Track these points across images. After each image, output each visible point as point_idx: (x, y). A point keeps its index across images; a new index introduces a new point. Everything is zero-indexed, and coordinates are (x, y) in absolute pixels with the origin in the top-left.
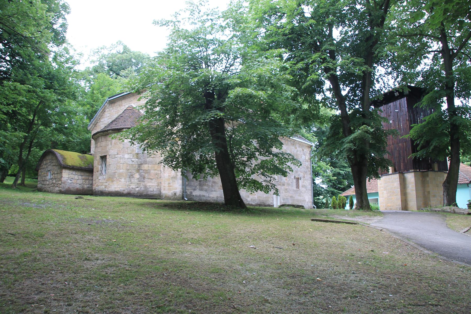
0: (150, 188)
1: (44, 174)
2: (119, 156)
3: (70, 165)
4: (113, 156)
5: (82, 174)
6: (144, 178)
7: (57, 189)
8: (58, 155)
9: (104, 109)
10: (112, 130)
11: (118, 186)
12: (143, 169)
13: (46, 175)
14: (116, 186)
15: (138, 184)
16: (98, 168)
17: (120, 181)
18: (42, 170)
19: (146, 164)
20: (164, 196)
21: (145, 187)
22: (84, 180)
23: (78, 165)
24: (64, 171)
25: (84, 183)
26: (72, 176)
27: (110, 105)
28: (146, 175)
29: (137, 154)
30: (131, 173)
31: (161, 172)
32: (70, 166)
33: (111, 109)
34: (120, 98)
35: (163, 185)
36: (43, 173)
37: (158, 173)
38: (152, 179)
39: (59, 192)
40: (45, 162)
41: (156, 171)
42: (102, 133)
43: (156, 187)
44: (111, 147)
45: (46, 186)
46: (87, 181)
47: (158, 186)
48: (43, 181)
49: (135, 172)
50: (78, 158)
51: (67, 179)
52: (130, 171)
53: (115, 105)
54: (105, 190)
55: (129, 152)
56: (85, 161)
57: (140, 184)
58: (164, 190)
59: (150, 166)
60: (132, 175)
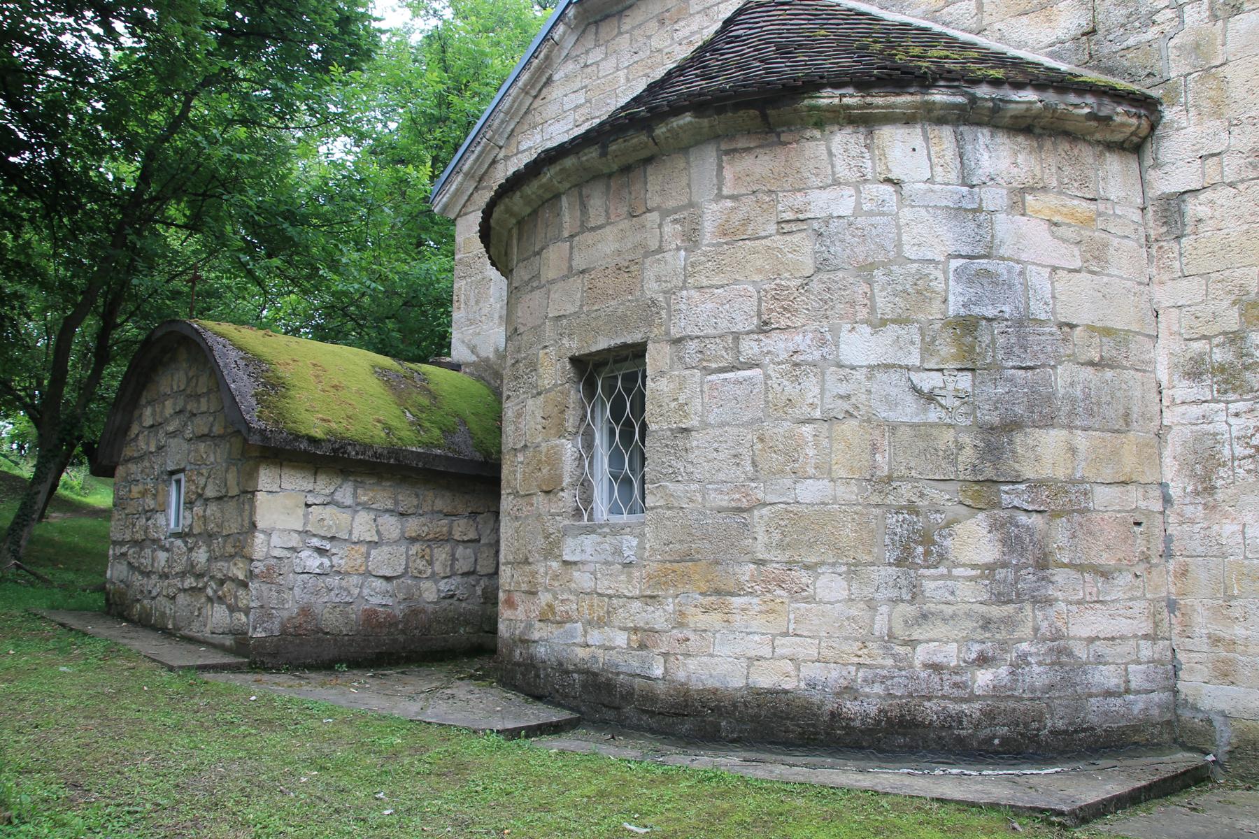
0: (1100, 660)
1: (144, 493)
2: (779, 344)
3: (318, 433)
4: (715, 348)
5: (407, 499)
6: (1043, 563)
7: (218, 616)
8: (228, 360)
9: (540, 70)
11: (786, 646)
12: (1029, 473)
13: (150, 503)
14: (756, 645)
15: (986, 624)
16: (554, 460)
18: (133, 467)
19: (1049, 422)
20: (1225, 737)
21: (1060, 654)
22: (415, 548)
23: (378, 435)
24: (266, 478)
25: (421, 564)
26: (333, 519)
27: (589, 41)
28: (1060, 535)
29: (967, 326)
30: (912, 509)
31: (1167, 500)
32: (313, 440)
33: (596, 55)
35: (1203, 624)
36: (136, 490)
37: (1149, 513)
38: (1105, 574)
39: (228, 641)
40: (148, 416)
41: (1134, 497)
42: (591, 155)
43: (1146, 650)
44: (690, 271)
45: (154, 584)
46: (441, 554)
47: (1152, 638)
48: (138, 544)
49: (953, 509)
50: (374, 385)
51: (294, 541)
52: (906, 492)
53: (627, 24)
54: (635, 665)
55: (884, 304)
56: (422, 409)
58: (1225, 673)
59: (1081, 440)
60: (926, 539)
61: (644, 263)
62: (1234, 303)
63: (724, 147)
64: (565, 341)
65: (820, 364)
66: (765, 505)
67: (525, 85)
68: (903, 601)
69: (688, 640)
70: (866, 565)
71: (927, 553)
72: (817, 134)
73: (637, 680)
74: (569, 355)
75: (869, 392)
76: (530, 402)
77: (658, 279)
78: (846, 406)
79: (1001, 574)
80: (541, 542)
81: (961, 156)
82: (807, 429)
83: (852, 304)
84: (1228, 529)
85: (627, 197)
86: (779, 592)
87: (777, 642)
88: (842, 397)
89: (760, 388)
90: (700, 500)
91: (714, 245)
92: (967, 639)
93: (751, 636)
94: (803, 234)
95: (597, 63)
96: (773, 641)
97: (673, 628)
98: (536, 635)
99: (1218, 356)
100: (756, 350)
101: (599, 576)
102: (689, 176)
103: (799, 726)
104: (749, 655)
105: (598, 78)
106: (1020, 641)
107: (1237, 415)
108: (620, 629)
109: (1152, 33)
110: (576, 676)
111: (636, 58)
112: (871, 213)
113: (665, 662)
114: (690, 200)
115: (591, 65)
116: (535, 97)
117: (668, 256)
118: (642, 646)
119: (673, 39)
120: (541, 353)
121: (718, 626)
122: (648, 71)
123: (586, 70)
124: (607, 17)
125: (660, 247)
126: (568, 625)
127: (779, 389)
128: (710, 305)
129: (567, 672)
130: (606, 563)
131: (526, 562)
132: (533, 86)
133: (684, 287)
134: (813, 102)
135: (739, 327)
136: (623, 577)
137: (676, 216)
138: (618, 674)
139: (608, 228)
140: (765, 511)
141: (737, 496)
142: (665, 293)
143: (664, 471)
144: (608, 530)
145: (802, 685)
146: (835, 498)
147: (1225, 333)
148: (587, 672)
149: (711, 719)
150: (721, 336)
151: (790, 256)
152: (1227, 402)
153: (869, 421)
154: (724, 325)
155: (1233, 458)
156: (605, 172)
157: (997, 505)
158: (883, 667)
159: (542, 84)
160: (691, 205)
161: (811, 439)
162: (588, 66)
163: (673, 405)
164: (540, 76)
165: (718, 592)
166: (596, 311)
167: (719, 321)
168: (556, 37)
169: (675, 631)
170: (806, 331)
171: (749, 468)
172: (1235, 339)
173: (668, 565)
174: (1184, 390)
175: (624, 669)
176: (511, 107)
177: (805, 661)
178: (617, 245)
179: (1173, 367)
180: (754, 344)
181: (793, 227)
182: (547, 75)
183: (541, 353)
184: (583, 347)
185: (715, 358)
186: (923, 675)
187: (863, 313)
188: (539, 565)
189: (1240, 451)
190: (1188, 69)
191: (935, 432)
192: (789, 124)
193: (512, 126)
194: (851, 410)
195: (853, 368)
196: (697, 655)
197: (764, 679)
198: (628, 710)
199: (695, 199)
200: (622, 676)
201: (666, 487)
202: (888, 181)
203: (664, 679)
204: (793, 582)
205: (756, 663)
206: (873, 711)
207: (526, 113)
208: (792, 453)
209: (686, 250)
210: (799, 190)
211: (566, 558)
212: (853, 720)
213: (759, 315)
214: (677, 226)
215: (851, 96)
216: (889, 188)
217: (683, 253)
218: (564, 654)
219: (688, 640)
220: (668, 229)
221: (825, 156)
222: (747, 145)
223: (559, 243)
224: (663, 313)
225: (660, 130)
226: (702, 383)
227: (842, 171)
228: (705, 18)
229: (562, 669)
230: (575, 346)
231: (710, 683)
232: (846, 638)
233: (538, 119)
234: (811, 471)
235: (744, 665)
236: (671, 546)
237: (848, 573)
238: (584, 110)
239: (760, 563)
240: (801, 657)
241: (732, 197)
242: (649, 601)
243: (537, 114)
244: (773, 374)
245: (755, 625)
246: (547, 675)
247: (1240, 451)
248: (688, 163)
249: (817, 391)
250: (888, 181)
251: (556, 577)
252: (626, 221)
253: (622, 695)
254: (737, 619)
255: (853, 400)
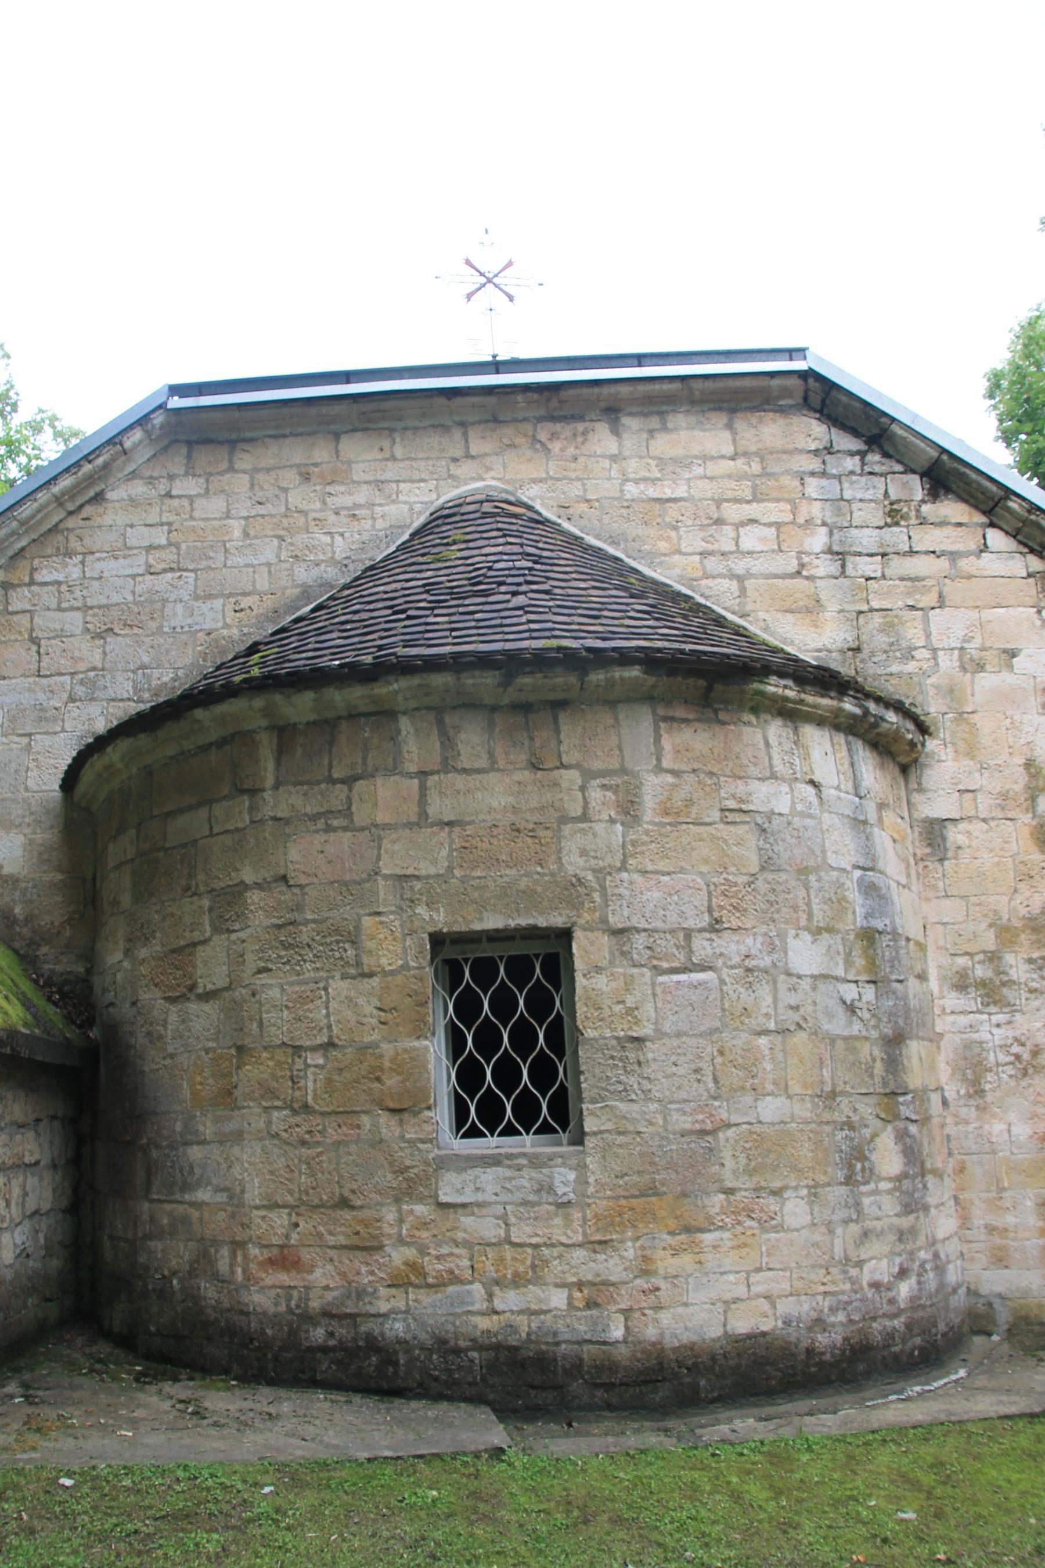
2: (731, 946)
4: (666, 944)
9: (91, 479)
10: (650, 660)
11: (761, 1283)
14: (731, 1286)
15: (902, 1235)
17: (769, 1223)
27: (176, 463)
30: (851, 1127)
34: (337, 409)
42: (485, 681)
53: (245, 461)
54: (583, 1329)
57: (913, 1231)
58: (1000, 1259)
60: (863, 1158)
61: (559, 830)
62: (990, 926)
63: (661, 711)
64: (422, 910)
65: (772, 971)
66: (729, 1126)
67: (63, 494)
68: (852, 1220)
69: (658, 1289)
70: (824, 1186)
71: (863, 1169)
72: (753, 719)
73: (586, 1348)
74: (431, 929)
75: (815, 1003)
76: (339, 987)
77: (583, 853)
78: (796, 1017)
79: (906, 1184)
80: (387, 1178)
81: (852, 765)
82: (763, 1041)
83: (795, 908)
84: (998, 1127)
85: (526, 743)
86: (749, 1223)
87: (752, 1280)
88: (791, 1008)
89: (715, 995)
90: (661, 1122)
91: (656, 824)
92: (892, 1254)
93: (725, 1277)
94: (746, 827)
95: (191, 499)
96: (747, 1279)
97: (636, 1277)
98: (383, 1307)
99: (981, 972)
100: (709, 951)
101: (513, 1220)
102: (619, 735)
103: (779, 1370)
104: (725, 1298)
105: (192, 518)
106: (920, 1249)
107: (998, 1026)
108: (557, 1285)
109: (911, 667)
110: (475, 1354)
111: (261, 510)
112: (803, 815)
113: (626, 1320)
114: (622, 764)
115: (180, 497)
116: (71, 513)
117: (599, 828)
118: (591, 1304)
119: (324, 503)
120: (367, 922)
121: (690, 1268)
122: (282, 533)
123: (168, 501)
124: (208, 441)
125: (584, 814)
126: (451, 1289)
127: (734, 996)
128: (656, 895)
129: (457, 1351)
130: (525, 1203)
131: (344, 1203)
132: (72, 498)
133: (623, 867)
134: (762, 687)
135: (690, 923)
136: (558, 1221)
137: (605, 781)
138: (557, 1344)
139: (493, 777)
140: (730, 1133)
141: (701, 1117)
142: (594, 871)
143: (612, 1088)
144: (525, 1162)
145: (780, 1323)
146: (792, 1117)
147: (984, 952)
148: (498, 1347)
149: (688, 1380)
150: (672, 931)
151: (735, 849)
152: (990, 1014)
153: (815, 1033)
154: (673, 920)
155: (998, 1065)
156: (486, 702)
157: (897, 1116)
158: (843, 1292)
159: (86, 498)
160: (623, 771)
161: (767, 1052)
162: (171, 497)
163: (617, 1008)
164: (87, 488)
165: (688, 1229)
166: (479, 878)
167: (667, 913)
168: (128, 444)
169: (638, 1281)
170: (755, 934)
171: (711, 1085)
172: (993, 958)
173: (623, 1202)
174: (953, 1000)
175: (567, 1337)
176: (33, 516)
177: (779, 1297)
178: (511, 800)
179: (942, 979)
180: (706, 944)
181: (737, 817)
182: (97, 489)
183: (367, 922)
184: (456, 921)
185: (666, 957)
186: (870, 1295)
187: (803, 922)
188: (384, 1210)
189: (1002, 1058)
190: (945, 709)
191: (858, 1044)
192: (726, 702)
193: (23, 543)
194: (801, 1022)
195: (799, 977)
196: (669, 1307)
197: (741, 1326)
198: (576, 1386)
199: (629, 765)
200: (563, 1346)
201: (616, 1107)
202: (812, 782)
203: (625, 1341)
204: (762, 1210)
205: (733, 1306)
206: (838, 1339)
207: (50, 530)
208: (750, 1068)
209: (623, 824)
210: (740, 778)
211: (443, 1199)
212: (823, 1354)
213: (710, 910)
214: (609, 794)
215: (791, 689)
216: (810, 790)
217: (619, 827)
218: (450, 1327)
219: (658, 1289)
220: (596, 795)
221: (762, 745)
222: (684, 716)
223: (397, 777)
224: (596, 896)
225: (597, 677)
226: (653, 984)
227: (779, 768)
228: (377, 493)
229: (443, 1346)
230: (441, 919)
231: (686, 1338)
232: (813, 1266)
233: (74, 544)
234: (770, 1087)
235: (721, 1310)
236: (626, 1178)
237: (810, 1194)
238: (170, 555)
239: (729, 1191)
240: (775, 1293)
241: (672, 772)
242: (597, 1247)
243: (72, 538)
244: (727, 980)
245: (728, 1263)
246: (412, 1360)
247: (1002, 1058)
248: (617, 720)
249: (769, 1000)
250: (812, 782)
251: (425, 1225)
252: (527, 773)
253: (565, 1370)
254: (709, 1258)
255: (802, 1010)
